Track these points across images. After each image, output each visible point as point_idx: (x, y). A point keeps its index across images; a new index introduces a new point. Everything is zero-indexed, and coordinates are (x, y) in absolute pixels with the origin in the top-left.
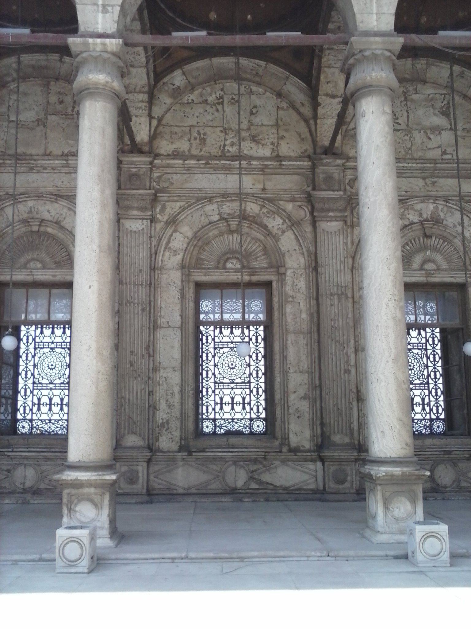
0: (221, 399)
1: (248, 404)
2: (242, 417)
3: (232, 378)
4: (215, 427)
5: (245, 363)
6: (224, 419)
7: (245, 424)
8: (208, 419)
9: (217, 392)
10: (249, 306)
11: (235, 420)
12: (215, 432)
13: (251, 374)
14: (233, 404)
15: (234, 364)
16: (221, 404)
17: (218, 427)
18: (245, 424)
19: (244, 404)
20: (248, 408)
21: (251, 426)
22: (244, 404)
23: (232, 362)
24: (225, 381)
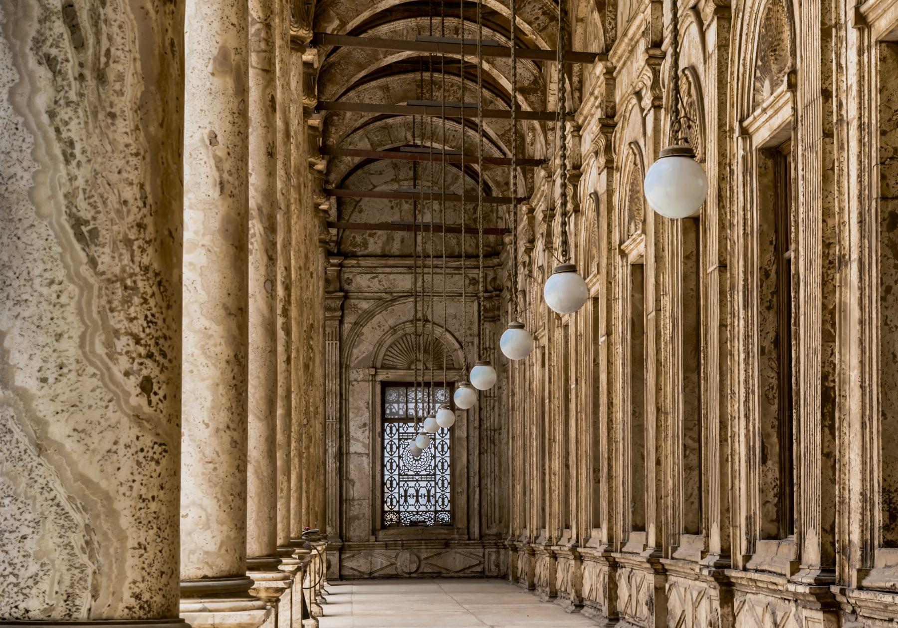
0: (406, 491)
8: (392, 511)
9: (401, 484)
10: (433, 395)
14: (417, 496)
16: (406, 496)
19: (429, 496)
22: (429, 496)
24: (410, 473)
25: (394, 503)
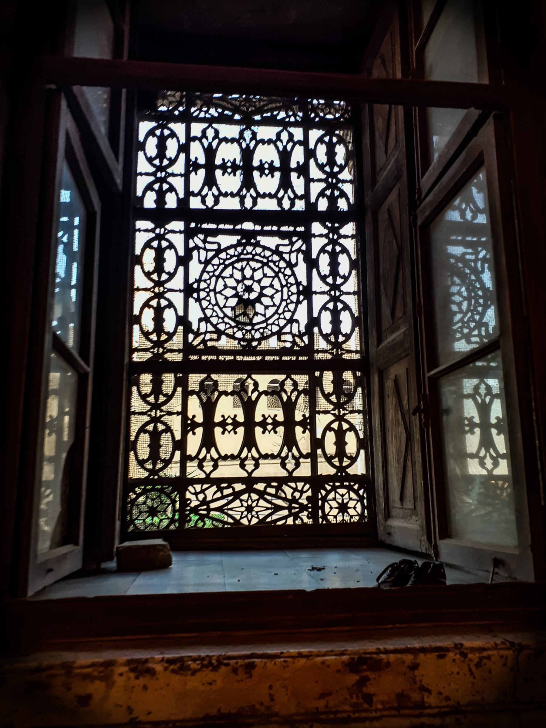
2: (284, 474)
6: (217, 482)
7: (294, 500)
11: (260, 486)
13: (314, 322)
15: (256, 287)
17: (195, 510)
18: (294, 500)
23: (248, 283)
25: (165, 451)
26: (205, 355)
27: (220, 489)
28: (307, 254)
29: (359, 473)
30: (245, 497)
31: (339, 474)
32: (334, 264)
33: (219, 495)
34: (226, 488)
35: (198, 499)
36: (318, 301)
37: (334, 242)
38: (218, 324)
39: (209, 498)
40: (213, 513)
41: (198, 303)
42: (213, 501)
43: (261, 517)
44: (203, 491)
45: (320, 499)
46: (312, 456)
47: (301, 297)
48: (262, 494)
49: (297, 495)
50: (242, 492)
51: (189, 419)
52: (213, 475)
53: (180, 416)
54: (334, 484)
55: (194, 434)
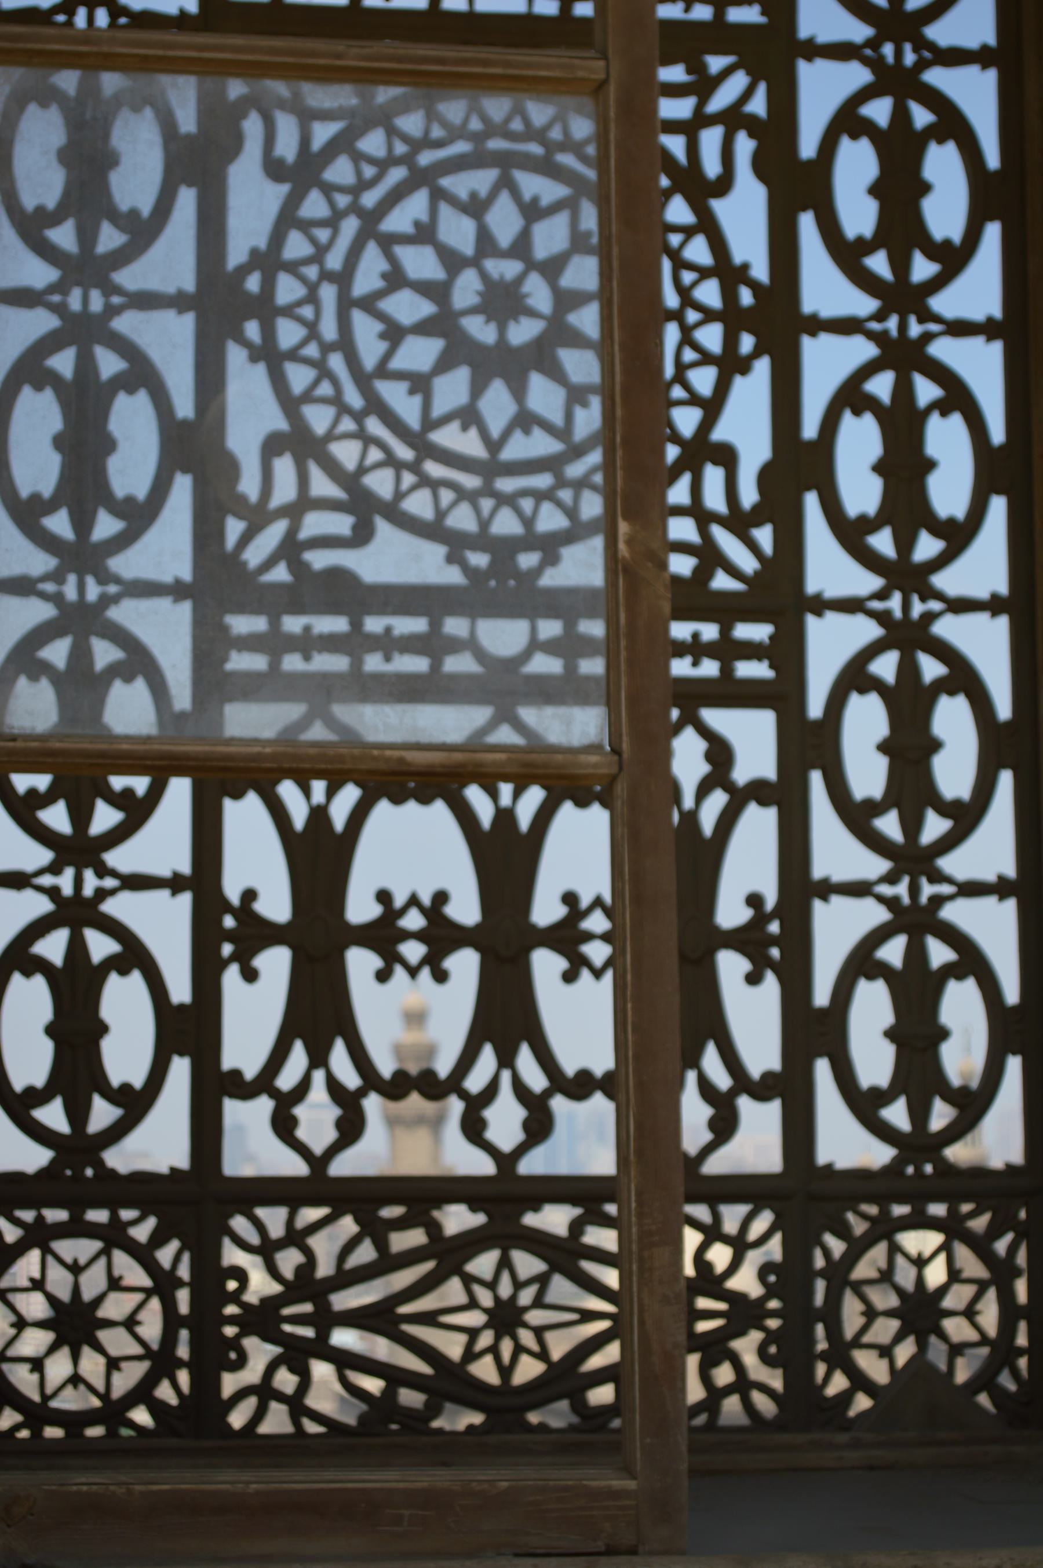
1: (748, 940)
3: (506, 524)
4: (204, 1320)
5: (709, 293)
6: (360, 1198)
11: (555, 1219)
12: (205, 1405)
13: (800, 465)
15: (538, 293)
17: (262, 1319)
20: (754, 1015)
21: (800, 1315)
24: (392, 558)
26: (298, 609)
27: (374, 1229)
28: (776, 133)
29: (997, 1163)
30: (483, 1264)
31: (910, 1170)
32: (900, 189)
33: (365, 1253)
34: (401, 1224)
35: (273, 1271)
36: (827, 364)
37: (894, 82)
38: (362, 470)
39: (324, 1269)
40: (344, 1338)
41: (261, 369)
42: (345, 1279)
43: (557, 1353)
44: (296, 1237)
45: (822, 1273)
46: (790, 1089)
47: (747, 343)
48: (564, 1255)
49: (720, 1256)
50: (472, 1243)
51: (226, 907)
52: (346, 1165)
53: (186, 899)
54: (885, 1212)
55: (250, 975)
